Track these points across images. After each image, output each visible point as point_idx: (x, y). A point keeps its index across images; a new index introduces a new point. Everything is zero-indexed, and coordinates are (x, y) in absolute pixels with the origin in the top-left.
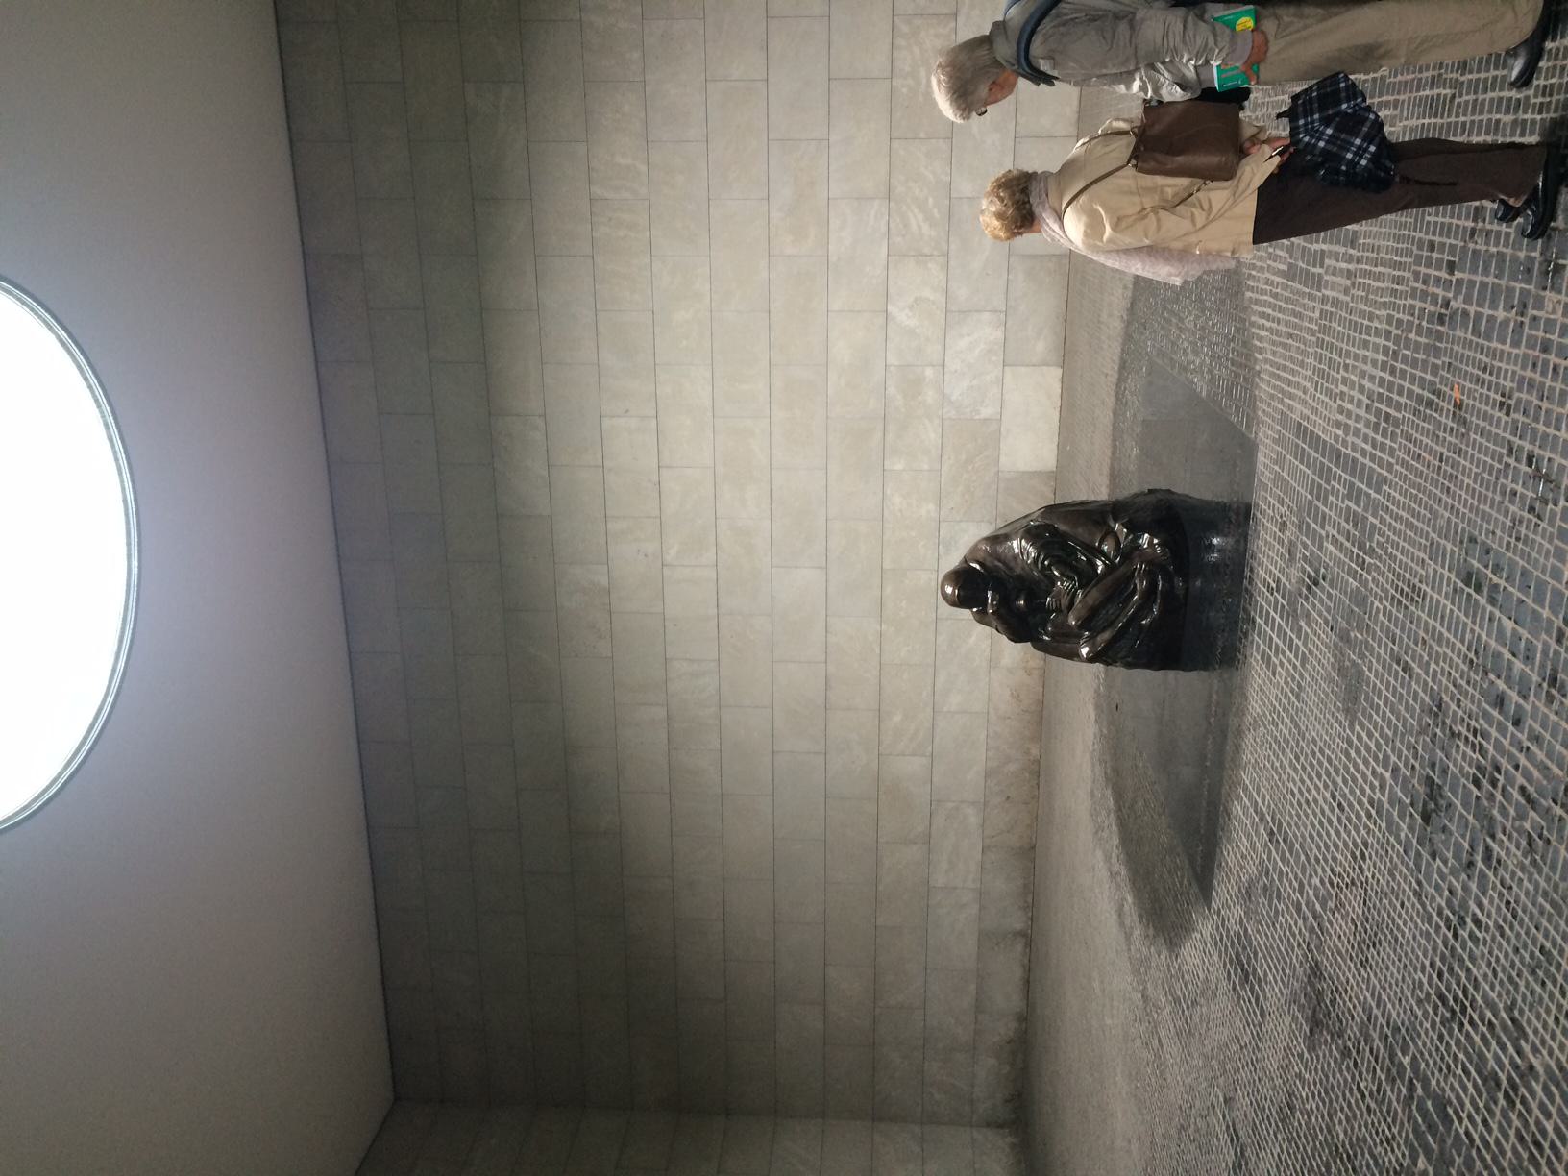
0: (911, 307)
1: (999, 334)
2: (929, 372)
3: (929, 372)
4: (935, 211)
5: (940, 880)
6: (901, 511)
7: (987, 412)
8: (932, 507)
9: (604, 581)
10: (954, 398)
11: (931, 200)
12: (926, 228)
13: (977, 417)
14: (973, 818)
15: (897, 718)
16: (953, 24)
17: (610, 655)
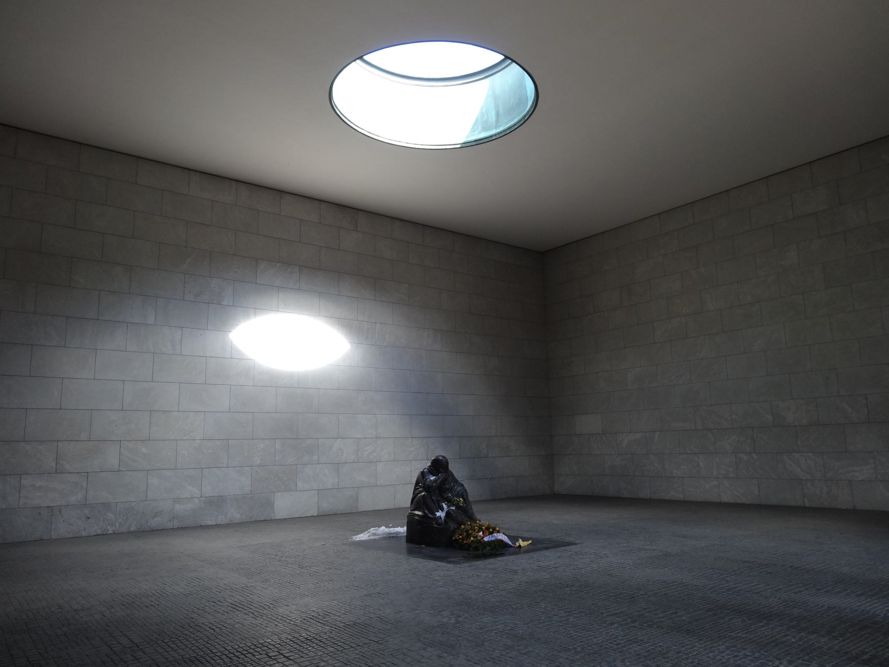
0: (340, 448)
1: (330, 486)
2: (316, 457)
3: (316, 457)
4: (372, 456)
5: (27, 481)
6: (257, 447)
7: (300, 484)
8: (258, 462)
9: (225, 303)
10: (305, 469)
11: (375, 454)
12: (366, 453)
13: (298, 480)
14: (73, 499)
15: (144, 450)
16: (425, 459)
17: (185, 299)
